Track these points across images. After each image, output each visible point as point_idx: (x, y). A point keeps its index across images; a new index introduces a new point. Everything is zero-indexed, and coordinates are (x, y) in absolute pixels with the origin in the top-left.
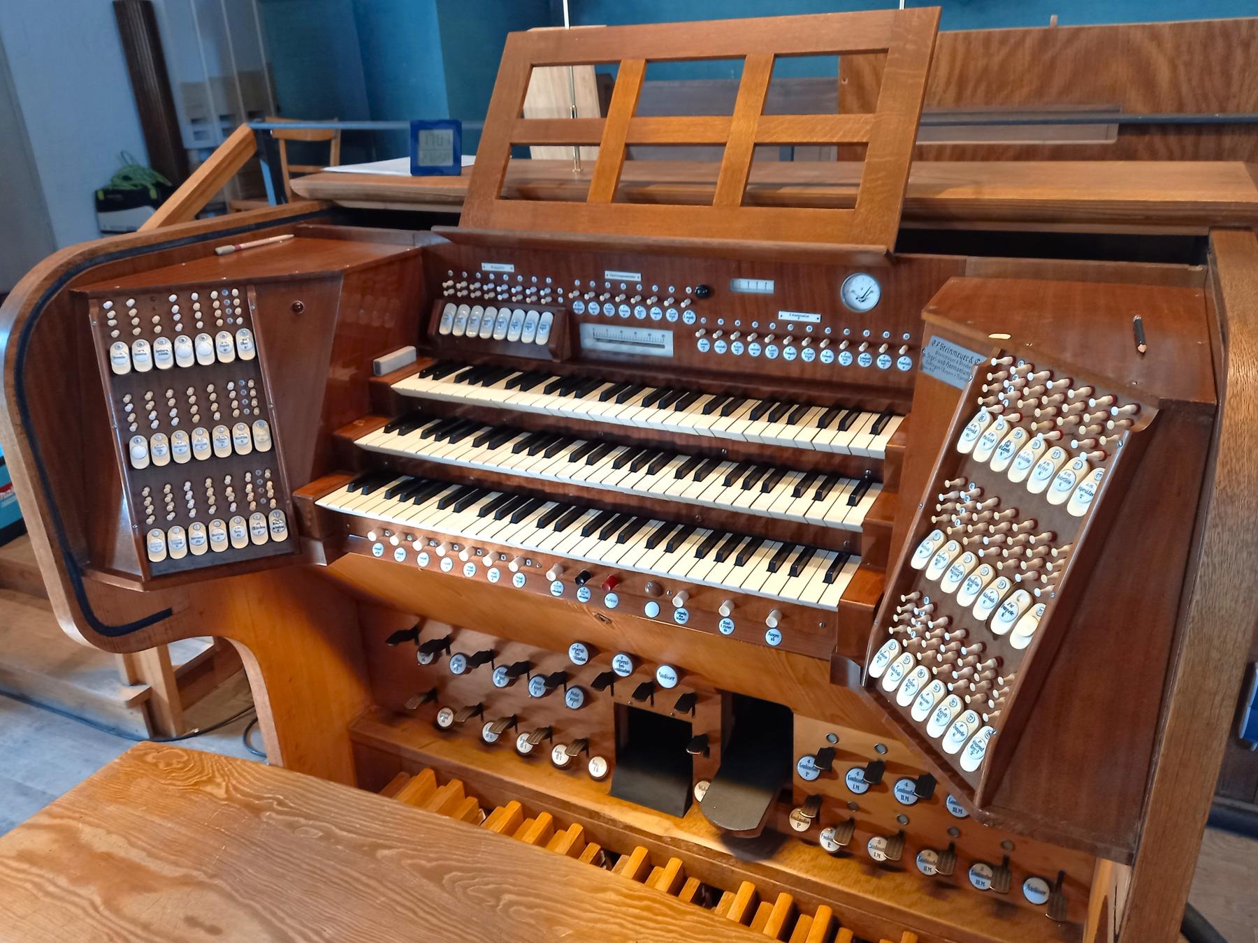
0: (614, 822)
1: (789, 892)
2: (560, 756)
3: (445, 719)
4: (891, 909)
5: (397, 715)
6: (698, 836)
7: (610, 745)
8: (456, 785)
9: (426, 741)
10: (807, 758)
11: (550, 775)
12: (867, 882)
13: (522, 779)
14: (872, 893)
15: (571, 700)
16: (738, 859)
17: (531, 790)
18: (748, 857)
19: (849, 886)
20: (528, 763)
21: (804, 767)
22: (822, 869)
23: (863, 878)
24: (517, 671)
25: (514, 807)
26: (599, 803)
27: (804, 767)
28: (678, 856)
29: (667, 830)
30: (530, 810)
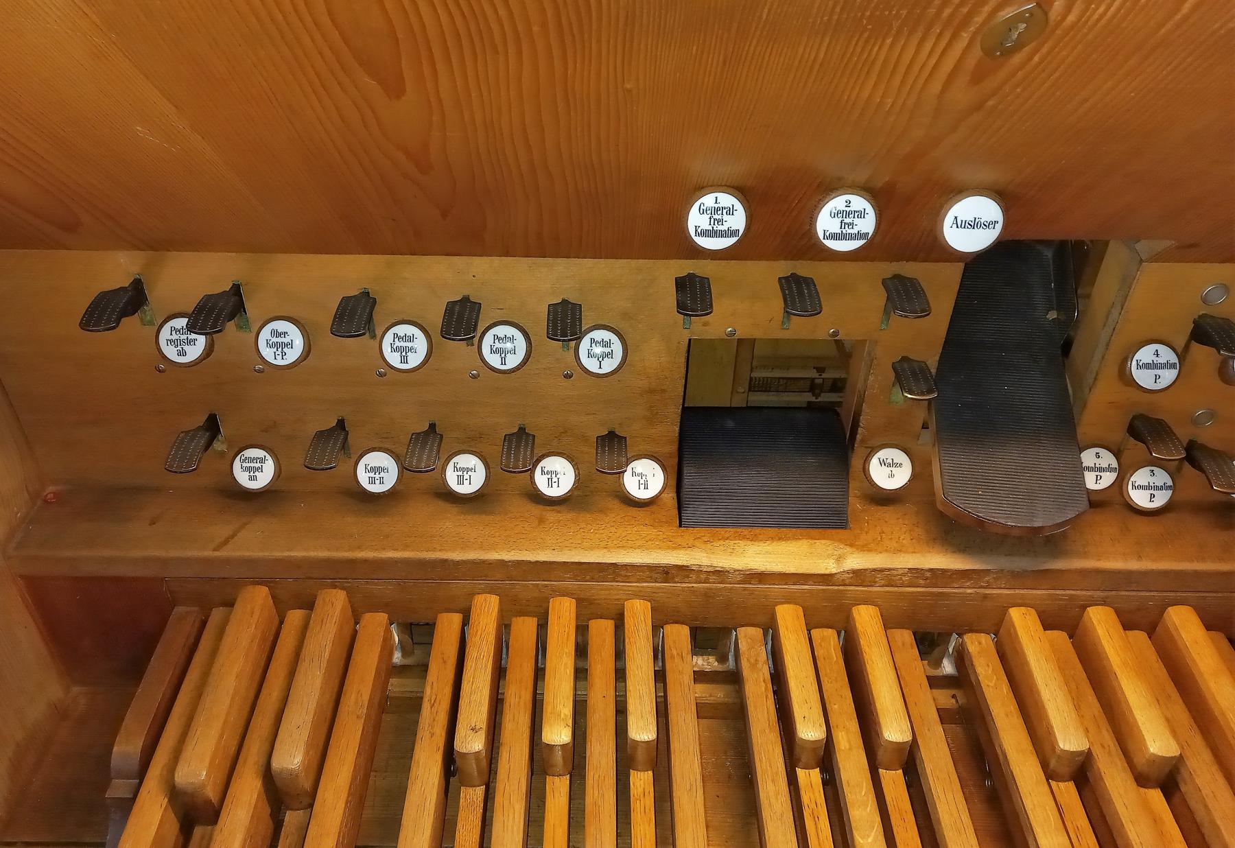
0: (720, 574)
2: (556, 476)
8: (334, 603)
9: (221, 530)
10: (1152, 348)
11: (541, 521)
13: (493, 547)
19: (1221, 560)
25: (487, 609)
28: (866, 601)
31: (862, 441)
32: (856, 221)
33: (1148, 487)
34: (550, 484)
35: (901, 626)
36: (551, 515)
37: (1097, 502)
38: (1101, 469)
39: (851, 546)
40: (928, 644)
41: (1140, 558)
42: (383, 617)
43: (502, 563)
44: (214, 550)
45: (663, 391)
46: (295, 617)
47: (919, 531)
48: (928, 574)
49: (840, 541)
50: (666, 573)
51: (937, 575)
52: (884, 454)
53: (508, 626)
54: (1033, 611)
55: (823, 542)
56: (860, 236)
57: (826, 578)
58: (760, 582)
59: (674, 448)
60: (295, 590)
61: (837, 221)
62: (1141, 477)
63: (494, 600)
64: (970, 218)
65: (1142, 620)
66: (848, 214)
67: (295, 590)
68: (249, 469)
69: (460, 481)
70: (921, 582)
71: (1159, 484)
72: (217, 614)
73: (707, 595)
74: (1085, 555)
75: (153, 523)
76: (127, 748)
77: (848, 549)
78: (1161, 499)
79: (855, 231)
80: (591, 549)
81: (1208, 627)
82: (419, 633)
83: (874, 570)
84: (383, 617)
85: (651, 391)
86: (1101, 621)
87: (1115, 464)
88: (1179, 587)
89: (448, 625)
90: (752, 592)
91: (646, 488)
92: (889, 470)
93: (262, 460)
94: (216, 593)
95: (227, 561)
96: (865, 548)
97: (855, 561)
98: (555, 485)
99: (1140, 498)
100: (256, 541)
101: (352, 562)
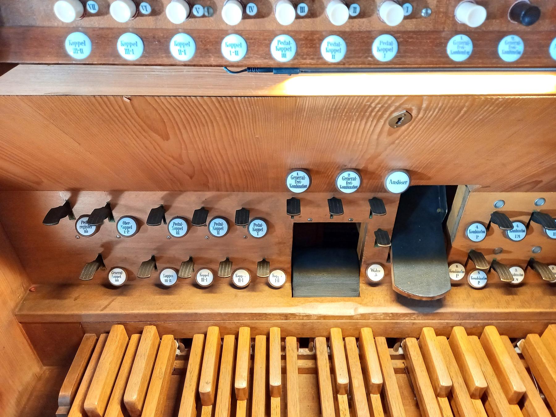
0: (308, 316)
1: (460, 325)
3: (118, 278)
4: (541, 313)
5: (62, 287)
6: (378, 306)
7: (288, 258)
8: (150, 332)
9: (104, 302)
11: (236, 296)
12: (513, 300)
14: (523, 307)
15: (256, 229)
16: (418, 315)
17: (226, 314)
18: (427, 310)
20: (211, 292)
21: (474, 232)
22: (481, 301)
23: (509, 298)
24: (200, 217)
25: (214, 333)
26: (292, 306)
27: (474, 232)
28: (367, 326)
29: (356, 309)
30: (225, 328)
31: (364, 262)
32: (353, 182)
33: (477, 279)
34: (239, 280)
35: (381, 335)
36: (239, 292)
37: (455, 284)
38: (458, 272)
39: (360, 304)
40: (392, 342)
41: (474, 307)
42: (171, 337)
43: (220, 314)
44: (102, 310)
45: (285, 243)
46: (135, 337)
47: (388, 297)
48: (391, 315)
49: (356, 302)
50: (286, 316)
51: (395, 316)
52: (373, 267)
53: (222, 339)
54: (432, 329)
55: (350, 303)
56: (354, 187)
57: (350, 317)
58: (324, 319)
59: (289, 265)
60: (134, 327)
61: (345, 182)
62: (474, 275)
63: (216, 329)
64: (396, 180)
65: (476, 331)
66: (349, 179)
67: (134, 327)
68: (115, 277)
69: (203, 280)
70: (388, 318)
71: (482, 277)
72: (102, 337)
73: (303, 325)
74: (452, 306)
75: (75, 299)
76: (65, 393)
77: (359, 305)
78: (482, 284)
79: (352, 185)
80: (256, 307)
81: (501, 334)
82: (187, 343)
83: (369, 314)
84: (171, 337)
85: (280, 243)
86: (459, 332)
87: (464, 270)
88: (490, 318)
89: (198, 340)
90: (321, 323)
91: (278, 281)
92: (375, 273)
93: (121, 273)
94: (103, 328)
95: (106, 315)
96: (366, 305)
97: (363, 310)
98: (241, 281)
99: (475, 283)
100: (119, 306)
101: (158, 315)
